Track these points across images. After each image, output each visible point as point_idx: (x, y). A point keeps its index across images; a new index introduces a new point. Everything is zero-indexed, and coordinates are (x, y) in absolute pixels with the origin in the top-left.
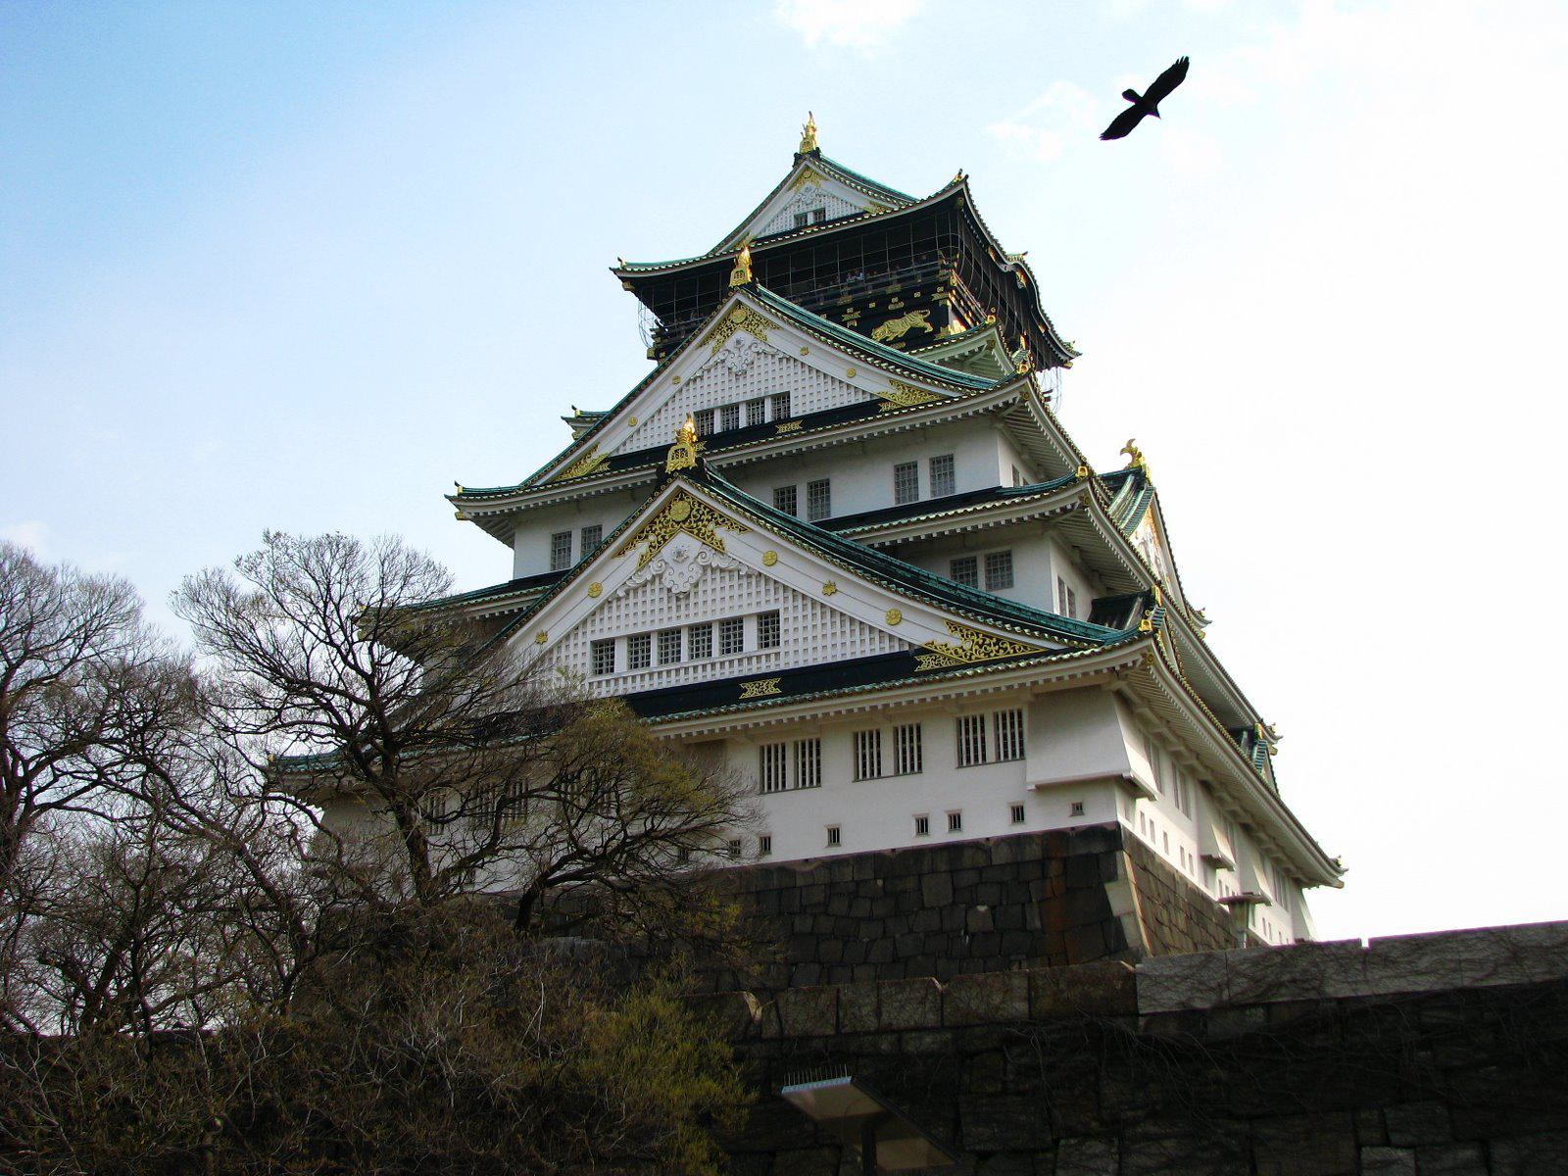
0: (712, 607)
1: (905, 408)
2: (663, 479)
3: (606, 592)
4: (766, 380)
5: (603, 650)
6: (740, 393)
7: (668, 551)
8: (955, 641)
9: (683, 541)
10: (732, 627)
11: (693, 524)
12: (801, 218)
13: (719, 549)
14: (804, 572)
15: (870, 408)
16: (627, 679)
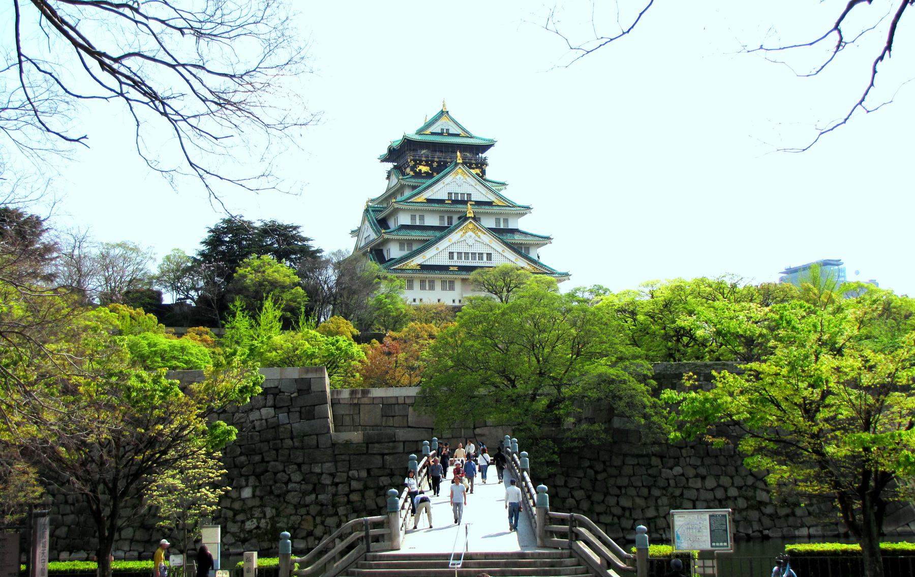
0: (478, 249)
1: (498, 206)
2: (466, 219)
3: (453, 241)
4: (465, 189)
5: (451, 254)
6: (459, 191)
7: (467, 235)
8: (528, 267)
9: (470, 233)
10: (481, 254)
11: (473, 230)
12: (442, 130)
13: (479, 237)
14: (498, 246)
15: (490, 204)
16: (456, 262)
